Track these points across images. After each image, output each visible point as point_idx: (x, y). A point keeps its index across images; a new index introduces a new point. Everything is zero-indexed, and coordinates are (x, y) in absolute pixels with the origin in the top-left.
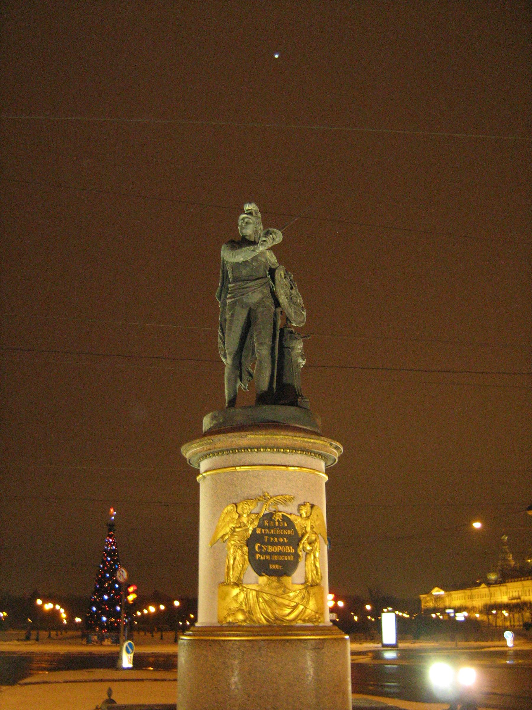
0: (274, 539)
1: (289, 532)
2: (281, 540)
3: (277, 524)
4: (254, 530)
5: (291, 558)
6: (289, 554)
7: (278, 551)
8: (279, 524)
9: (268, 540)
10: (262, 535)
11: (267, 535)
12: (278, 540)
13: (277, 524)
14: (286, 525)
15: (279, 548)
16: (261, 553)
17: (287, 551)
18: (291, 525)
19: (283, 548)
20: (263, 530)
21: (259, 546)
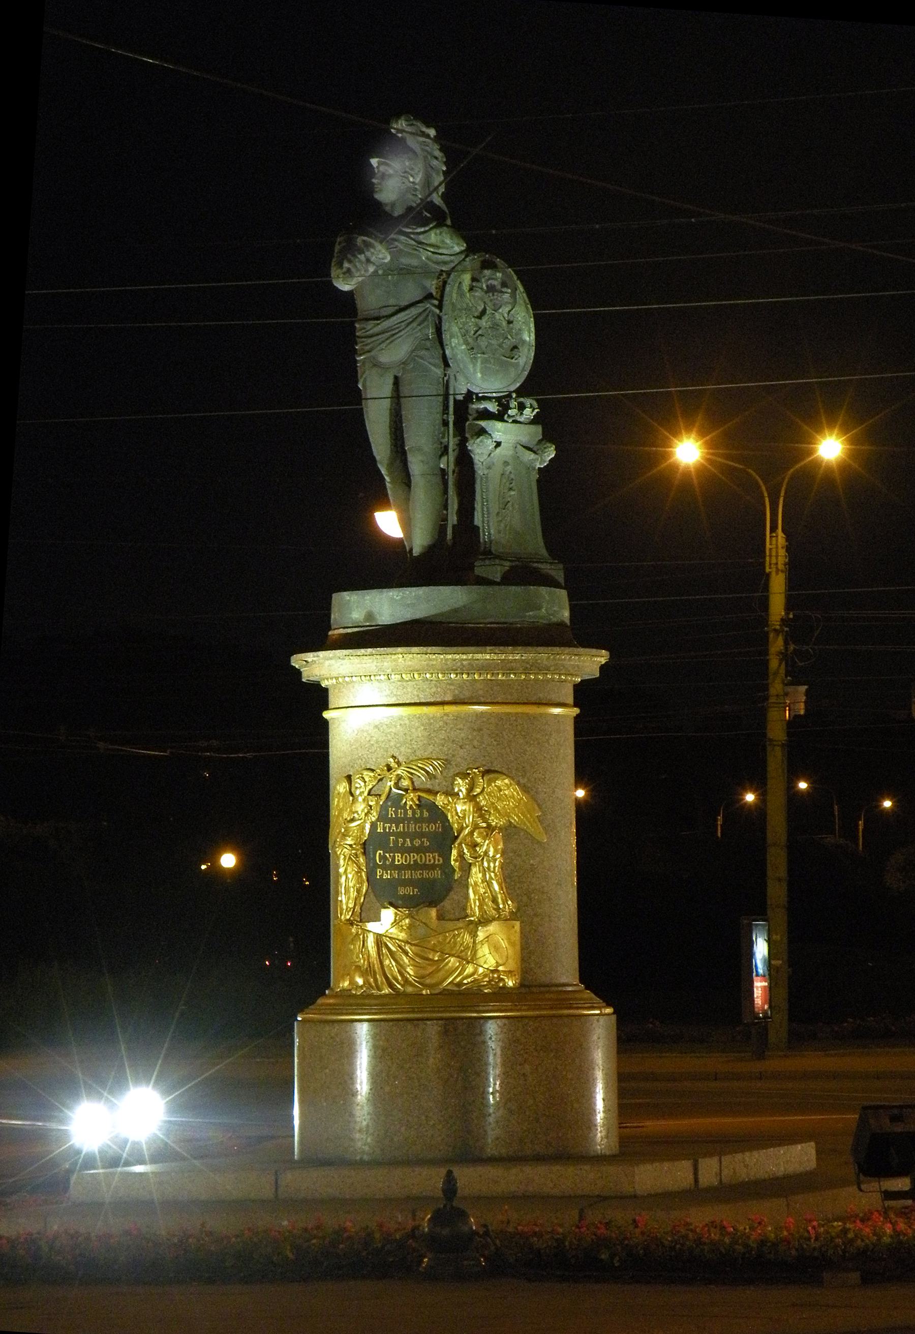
0: (405, 841)
1: (433, 828)
2: (417, 843)
3: (410, 813)
4: (373, 825)
5: (437, 874)
6: (433, 867)
7: (412, 863)
8: (414, 813)
9: (396, 842)
10: (386, 835)
11: (393, 834)
12: (411, 842)
13: (410, 813)
14: (426, 814)
15: (414, 856)
16: (384, 868)
17: (427, 862)
18: (438, 815)
19: (421, 856)
20: (387, 825)
21: (380, 853)
